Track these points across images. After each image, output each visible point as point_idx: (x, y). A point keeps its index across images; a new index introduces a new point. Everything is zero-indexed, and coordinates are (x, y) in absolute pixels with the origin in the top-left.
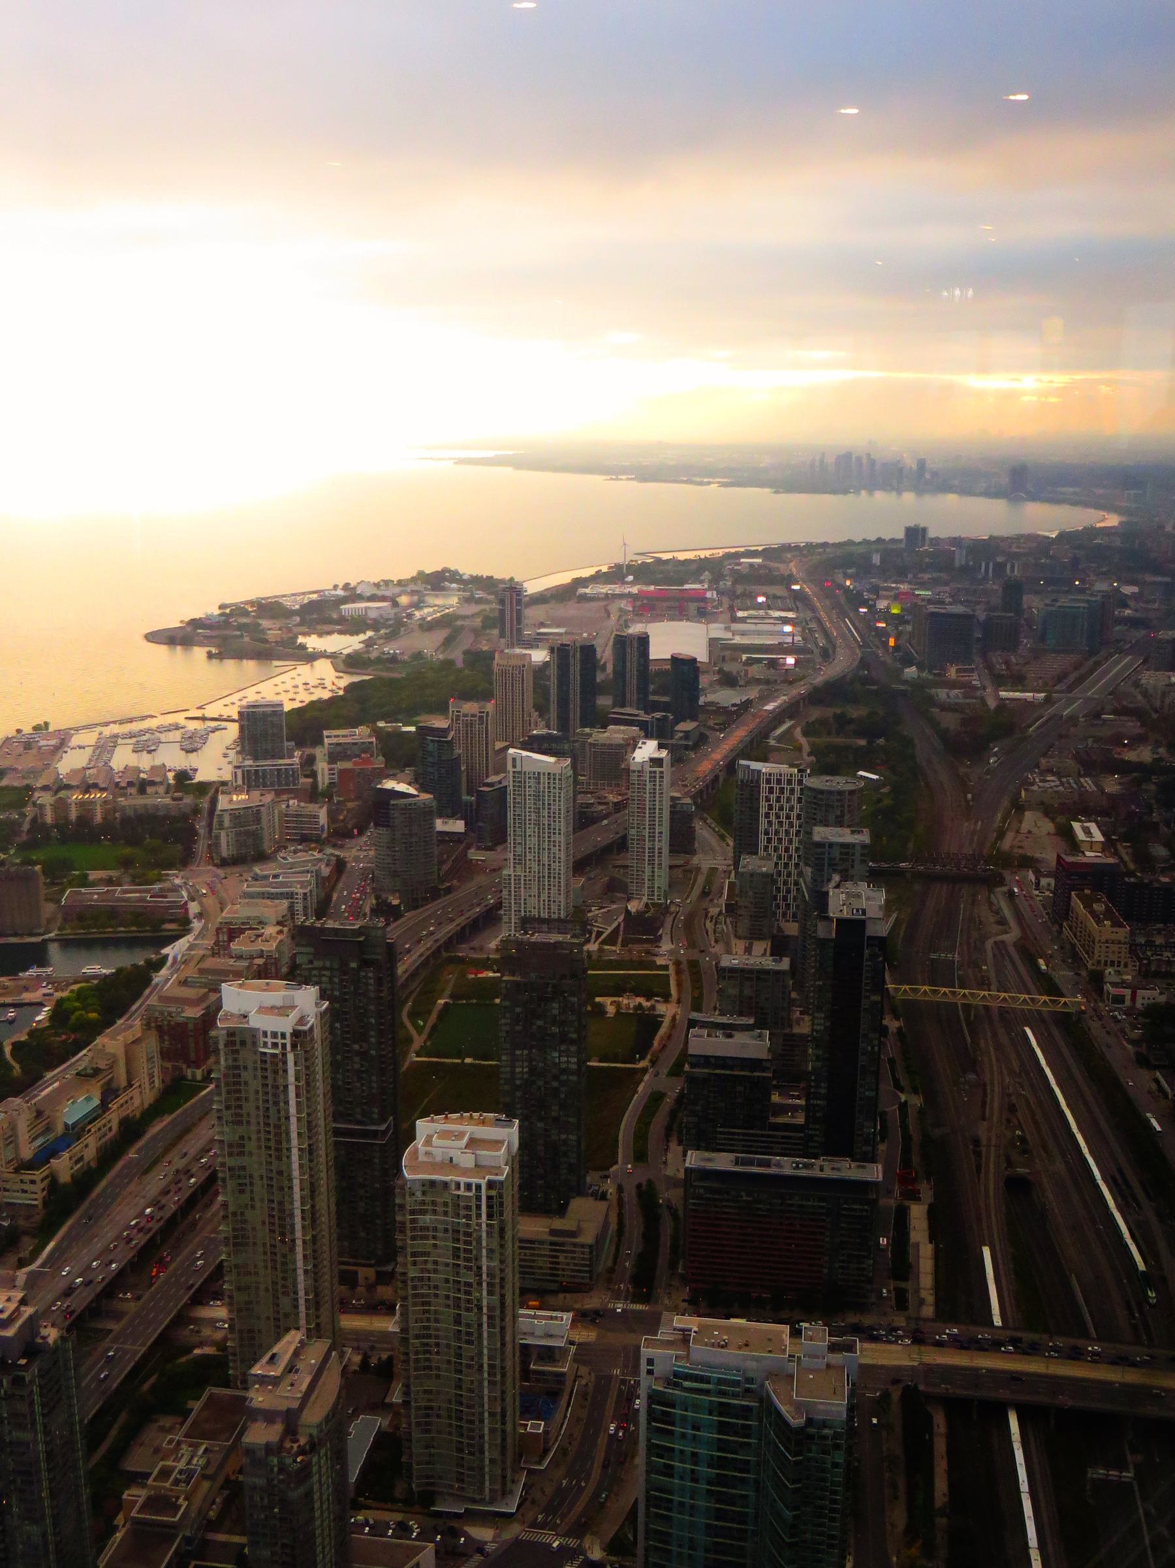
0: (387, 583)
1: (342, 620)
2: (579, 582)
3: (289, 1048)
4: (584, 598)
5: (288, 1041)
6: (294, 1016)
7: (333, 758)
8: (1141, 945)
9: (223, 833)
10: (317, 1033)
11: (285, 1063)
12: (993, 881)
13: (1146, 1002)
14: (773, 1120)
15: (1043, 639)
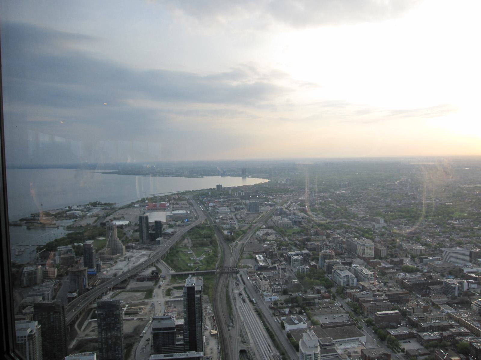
0: (80, 206)
1: (67, 216)
2: (133, 203)
3: (27, 340)
4: (134, 207)
5: (27, 338)
6: (29, 331)
7: (59, 255)
8: (272, 285)
9: (25, 278)
10: (36, 335)
11: (25, 345)
12: (237, 272)
13: (274, 299)
14: (177, 343)
15: (249, 211)
